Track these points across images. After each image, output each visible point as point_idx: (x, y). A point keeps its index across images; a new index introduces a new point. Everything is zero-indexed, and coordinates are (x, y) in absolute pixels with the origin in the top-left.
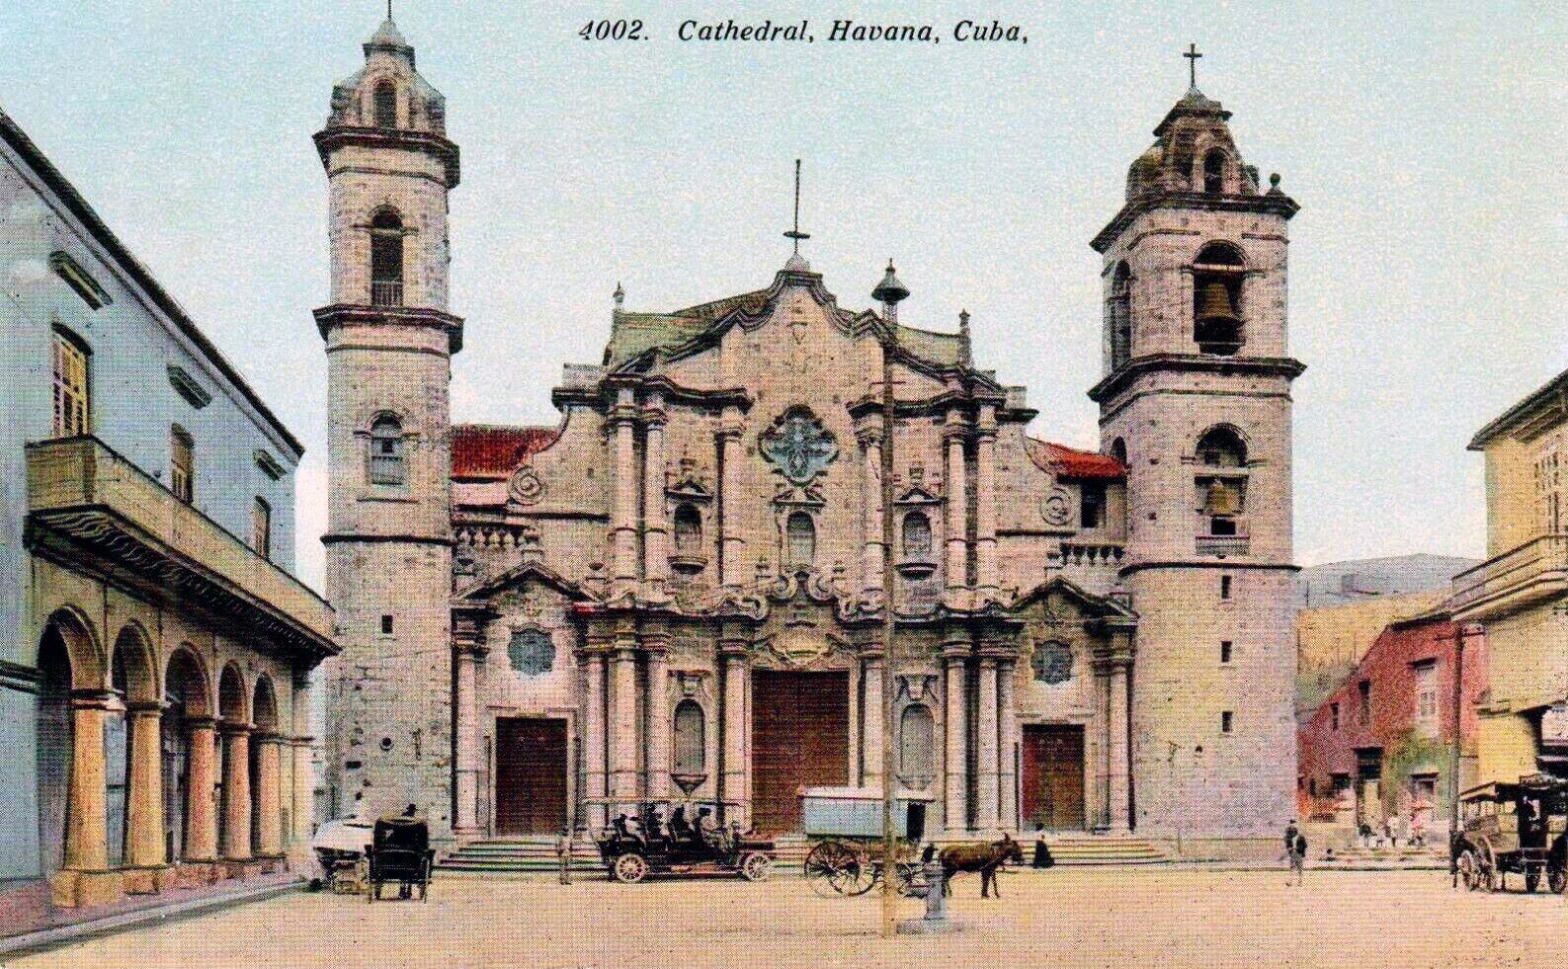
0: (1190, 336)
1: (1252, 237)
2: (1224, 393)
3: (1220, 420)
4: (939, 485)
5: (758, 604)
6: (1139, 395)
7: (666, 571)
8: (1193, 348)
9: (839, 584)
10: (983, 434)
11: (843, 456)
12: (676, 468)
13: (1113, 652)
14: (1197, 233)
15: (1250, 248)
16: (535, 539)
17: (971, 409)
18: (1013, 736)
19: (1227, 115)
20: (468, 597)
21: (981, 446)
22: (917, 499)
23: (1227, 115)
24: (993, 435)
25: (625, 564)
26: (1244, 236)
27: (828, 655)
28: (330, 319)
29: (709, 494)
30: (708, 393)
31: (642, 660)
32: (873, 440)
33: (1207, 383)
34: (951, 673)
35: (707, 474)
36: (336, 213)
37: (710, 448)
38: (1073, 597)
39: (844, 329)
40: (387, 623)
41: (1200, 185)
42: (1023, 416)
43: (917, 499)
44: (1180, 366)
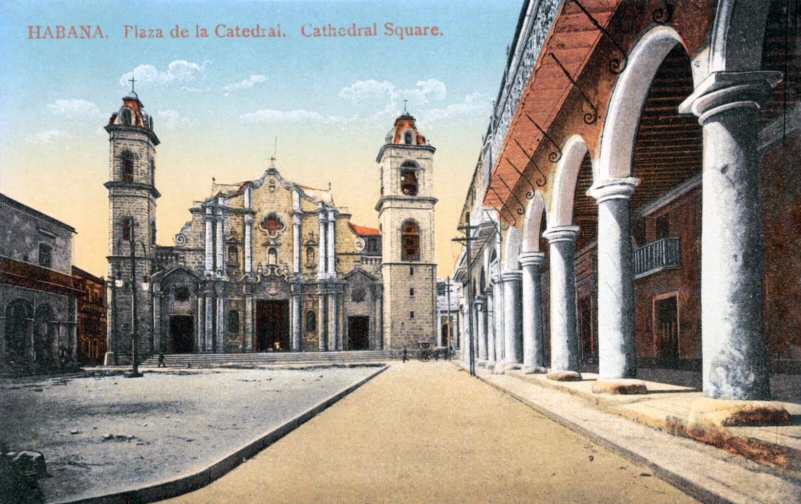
0: (399, 190)
8: (400, 194)
11: (287, 230)
15: (419, 162)
25: (209, 266)
26: (418, 158)
28: (109, 185)
38: (365, 273)
41: (402, 141)
43: (311, 243)
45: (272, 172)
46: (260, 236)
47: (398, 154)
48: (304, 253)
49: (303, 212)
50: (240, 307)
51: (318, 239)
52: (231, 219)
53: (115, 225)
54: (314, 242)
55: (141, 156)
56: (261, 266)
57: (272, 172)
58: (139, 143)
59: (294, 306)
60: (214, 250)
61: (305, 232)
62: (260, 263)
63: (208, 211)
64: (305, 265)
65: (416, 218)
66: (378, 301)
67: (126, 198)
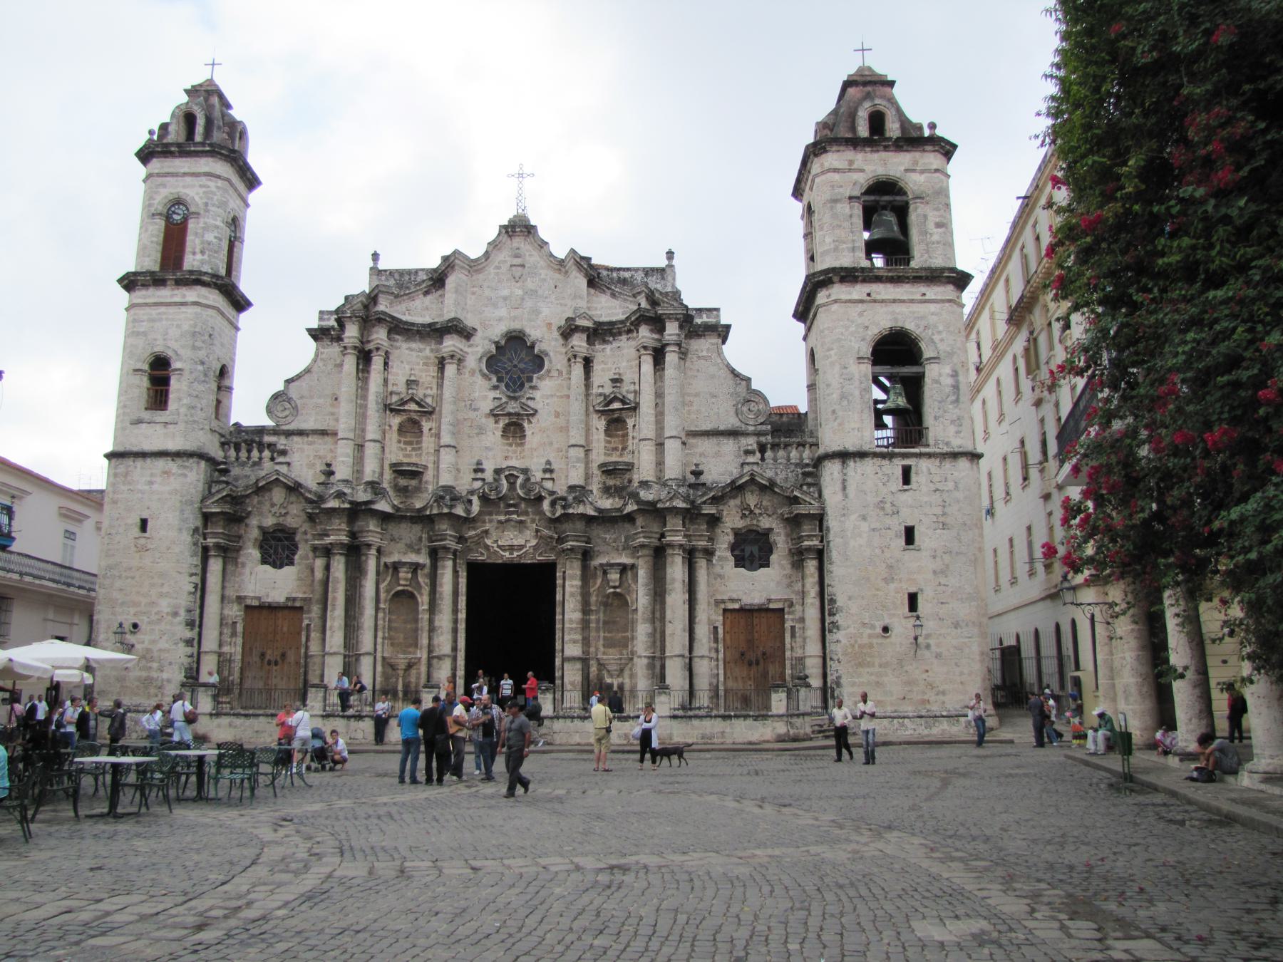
0: (863, 255)
1: (914, 171)
2: (894, 301)
4: (635, 392)
5: (470, 502)
7: (388, 475)
9: (548, 485)
10: (668, 344)
11: (555, 374)
12: (402, 388)
13: (800, 539)
14: (862, 171)
16: (283, 453)
17: (658, 324)
18: (707, 616)
19: (891, 84)
20: (217, 501)
22: (616, 405)
23: (891, 84)
24: (679, 345)
27: (535, 548)
29: (430, 409)
30: (430, 325)
31: (354, 551)
32: (575, 356)
33: (879, 293)
35: (429, 392)
36: (147, 206)
37: (433, 370)
39: (556, 267)
40: (144, 524)
41: (863, 131)
42: (723, 332)
43: (616, 405)
44: (849, 276)
45: (519, 229)
46: (484, 394)
47: (851, 162)
48: (599, 437)
49: (595, 323)
50: (423, 580)
52: (410, 349)
53: (131, 370)
54: (623, 401)
55: (207, 211)
56: (482, 471)
57: (519, 229)
58: (203, 180)
59: (569, 585)
60: (361, 428)
61: (601, 377)
62: (479, 463)
63: (352, 331)
64: (601, 466)
65: (910, 326)
66: (811, 565)
67: (163, 309)
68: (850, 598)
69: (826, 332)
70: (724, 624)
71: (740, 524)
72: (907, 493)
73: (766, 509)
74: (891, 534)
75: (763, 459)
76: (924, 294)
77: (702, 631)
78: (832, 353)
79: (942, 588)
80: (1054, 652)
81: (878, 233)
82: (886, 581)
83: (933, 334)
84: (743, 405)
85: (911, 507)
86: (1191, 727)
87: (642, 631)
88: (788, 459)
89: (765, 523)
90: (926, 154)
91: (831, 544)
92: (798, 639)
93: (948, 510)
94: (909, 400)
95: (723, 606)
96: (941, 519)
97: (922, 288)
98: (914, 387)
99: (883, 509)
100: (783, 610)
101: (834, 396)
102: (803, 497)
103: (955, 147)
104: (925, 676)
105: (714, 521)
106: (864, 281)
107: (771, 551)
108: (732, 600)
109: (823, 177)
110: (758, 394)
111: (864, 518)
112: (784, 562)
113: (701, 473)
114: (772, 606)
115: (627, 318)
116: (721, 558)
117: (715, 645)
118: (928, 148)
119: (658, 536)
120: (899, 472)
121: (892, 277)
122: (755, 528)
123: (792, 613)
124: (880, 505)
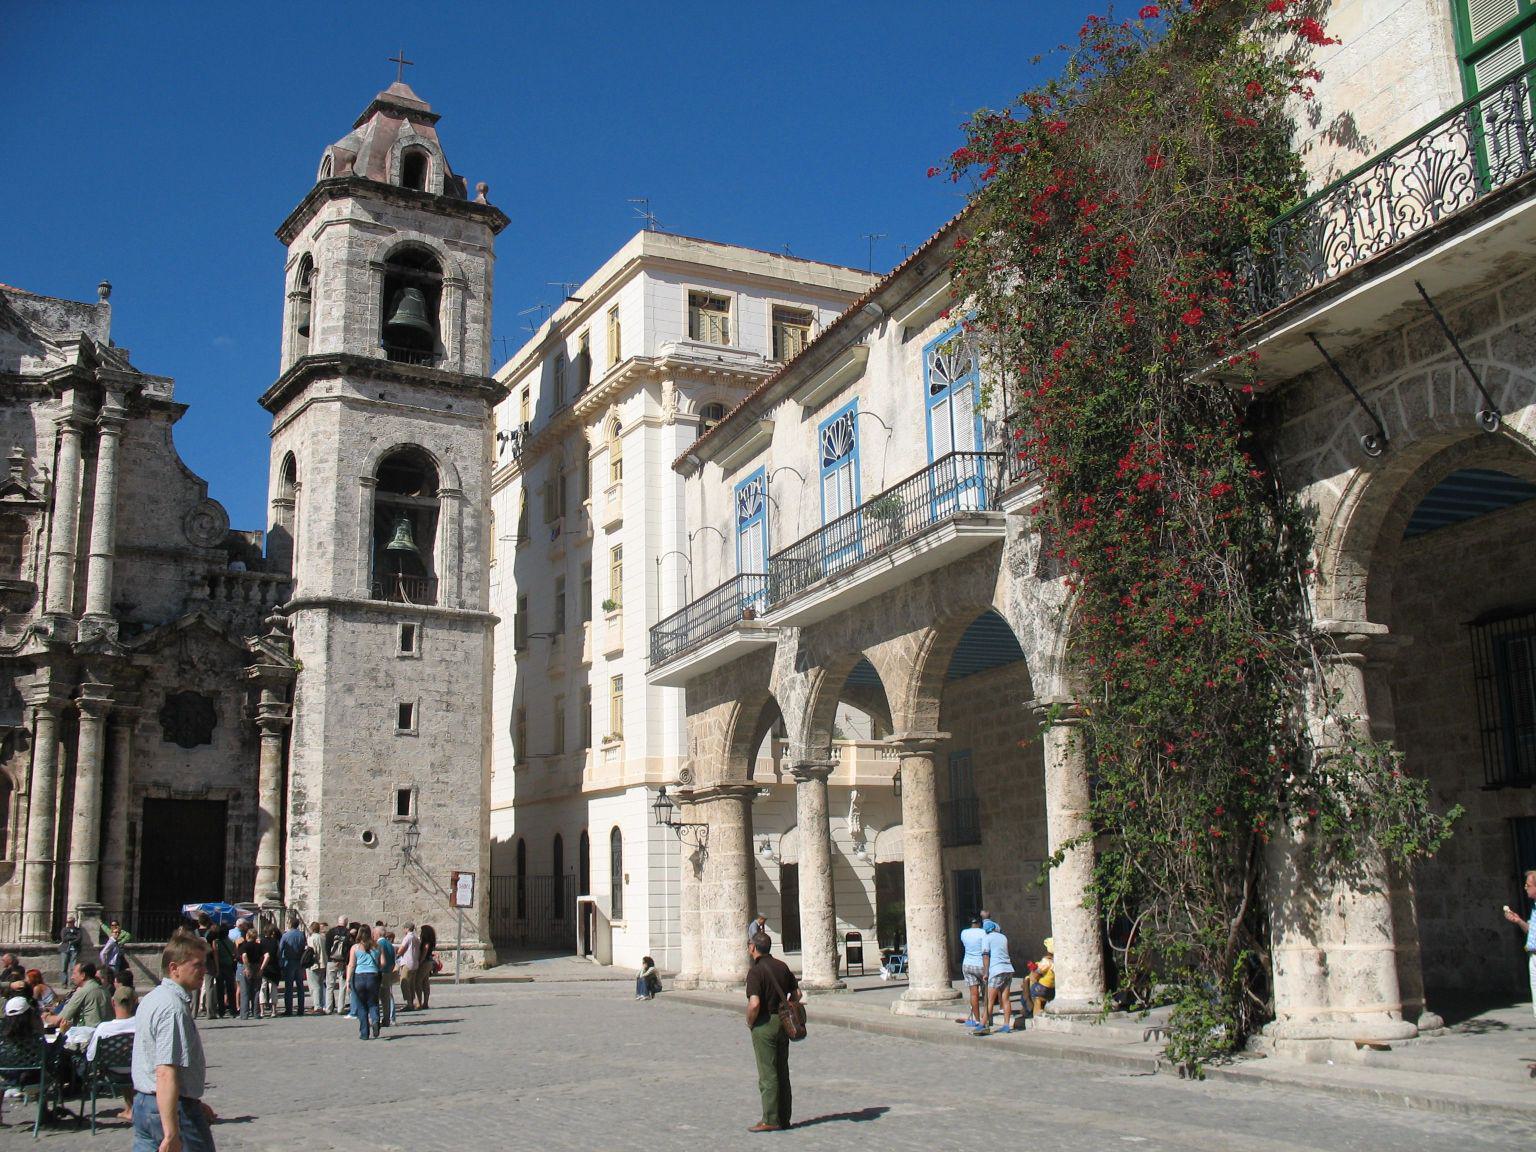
3: (404, 439)
6: (314, 400)
8: (381, 354)
14: (393, 231)
18: (124, 806)
21: (103, 437)
22: (16, 498)
24: (121, 425)
33: (394, 396)
34: (39, 725)
41: (397, 182)
42: (174, 411)
43: (16, 498)
51: (51, 487)
65: (428, 444)
68: (325, 793)
69: (321, 436)
70: (144, 820)
71: (175, 683)
72: (407, 662)
73: (213, 664)
74: (382, 712)
75: (212, 595)
76: (450, 407)
77: (120, 829)
78: (324, 465)
79: (443, 786)
80: (549, 869)
81: (400, 317)
82: (376, 772)
83: (455, 459)
84: (194, 519)
85: (410, 679)
86: (818, 960)
87: (36, 824)
88: (247, 599)
89: (210, 684)
90: (472, 224)
91: (304, 720)
92: (244, 844)
93: (455, 688)
94: (415, 542)
95: (144, 794)
96: (445, 698)
97: (449, 400)
98: (424, 525)
99: (375, 679)
100: (227, 801)
101: (324, 523)
102: (271, 654)
103: (507, 221)
104: (413, 897)
105: (146, 674)
106: (378, 377)
107: (214, 724)
108: (156, 784)
109: (340, 228)
110: (215, 504)
111: (350, 689)
112: (231, 738)
113: (133, 607)
114: (213, 797)
115: (47, 375)
116: (145, 728)
117: (131, 848)
118: (478, 217)
119: (69, 692)
120: (398, 631)
121: (414, 378)
122: (196, 689)
123: (240, 807)
124: (372, 674)
